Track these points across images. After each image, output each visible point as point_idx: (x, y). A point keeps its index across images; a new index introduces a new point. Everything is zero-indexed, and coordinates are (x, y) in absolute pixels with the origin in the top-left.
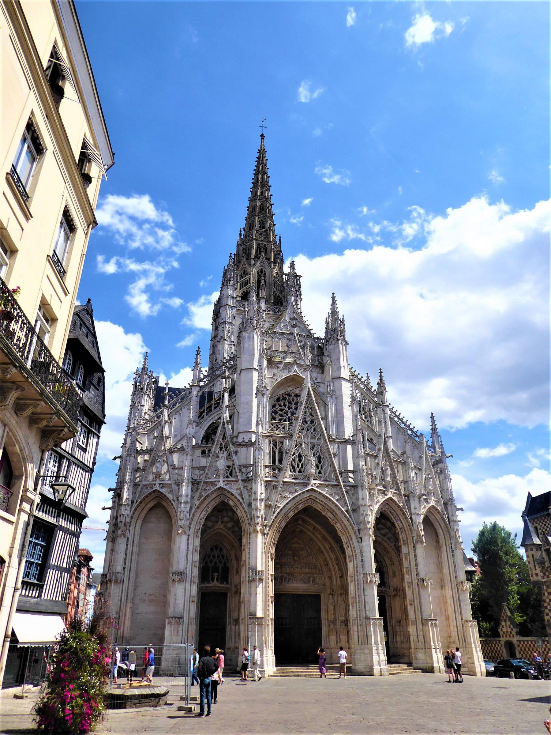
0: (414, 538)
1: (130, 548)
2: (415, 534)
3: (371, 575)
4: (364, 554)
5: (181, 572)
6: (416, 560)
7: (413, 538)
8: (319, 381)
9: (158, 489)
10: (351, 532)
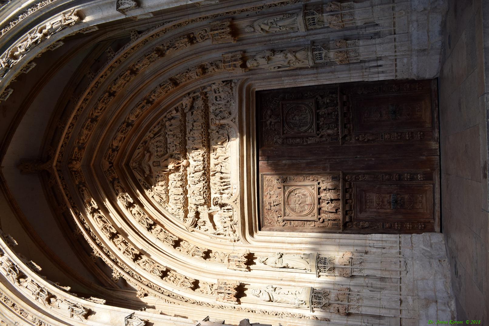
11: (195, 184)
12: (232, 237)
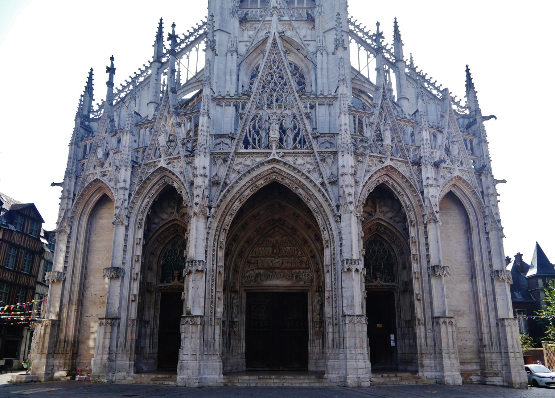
0: (426, 217)
1: (73, 246)
2: (427, 212)
3: (349, 262)
4: (344, 237)
5: (118, 268)
6: (427, 244)
7: (424, 216)
8: (308, 38)
9: (99, 178)
10: (328, 211)
11: (267, 263)
12: (243, 281)
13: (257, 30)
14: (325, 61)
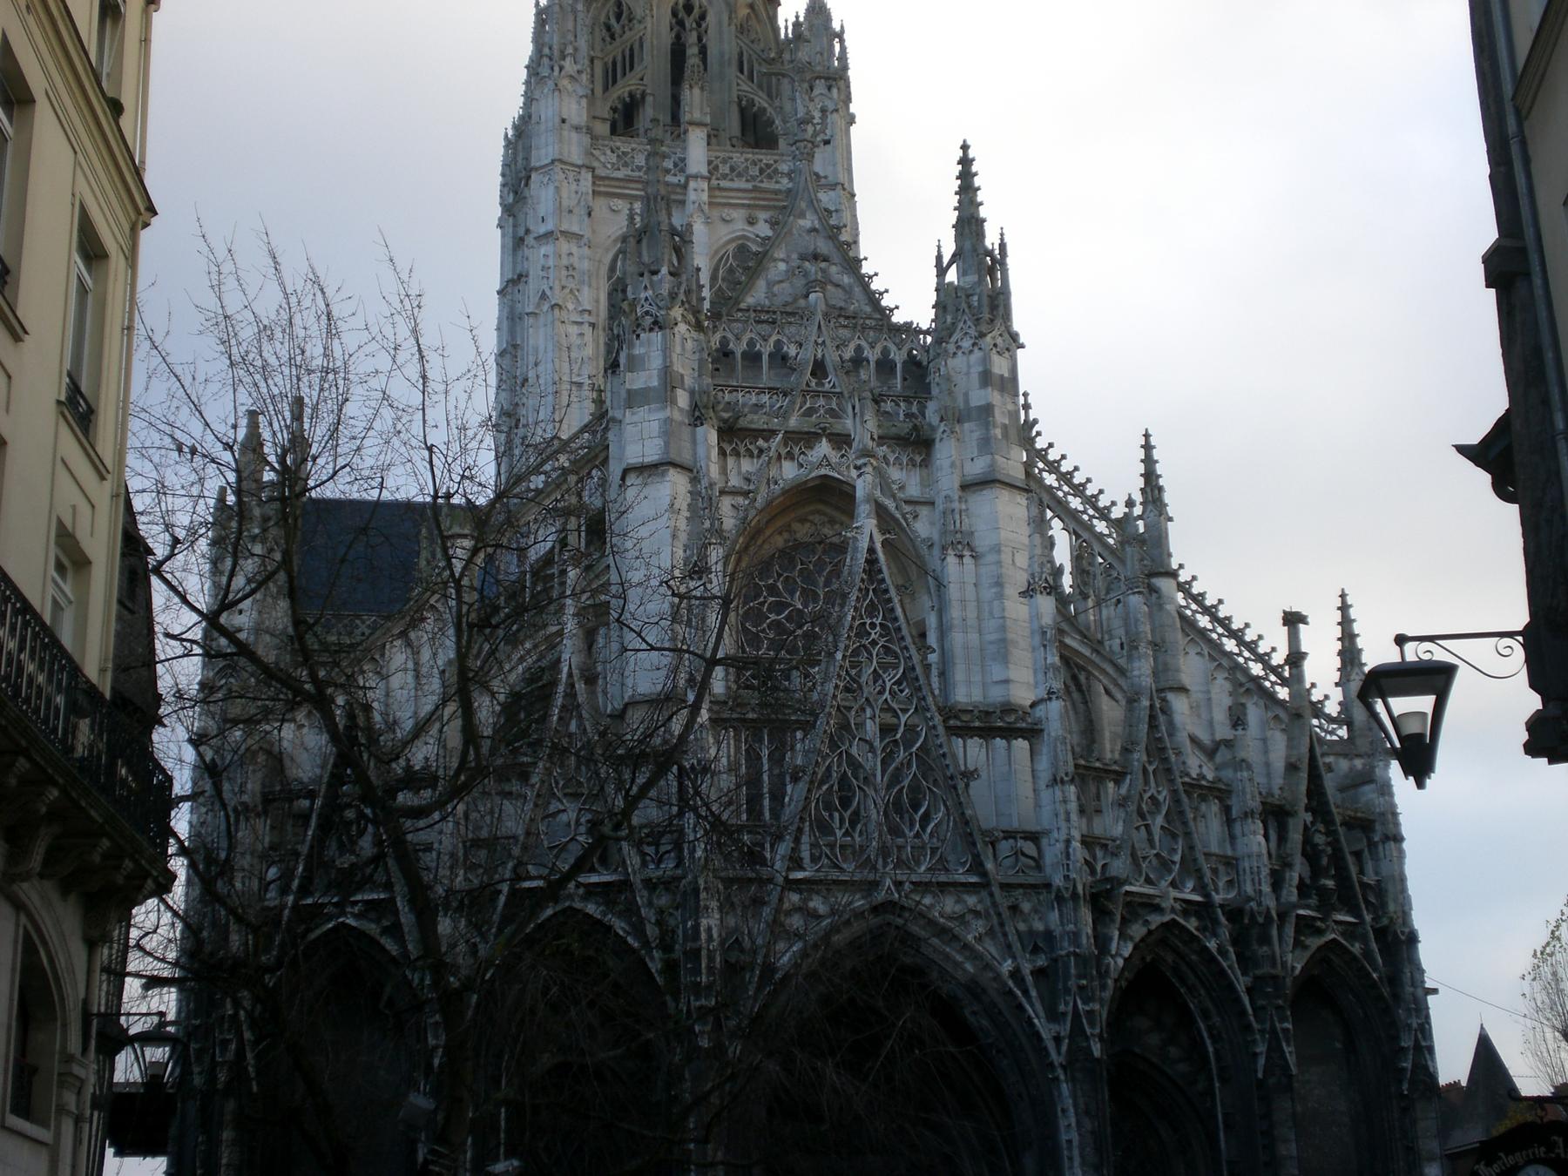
0: (1262, 1061)
13: (764, 458)
14: (970, 579)
